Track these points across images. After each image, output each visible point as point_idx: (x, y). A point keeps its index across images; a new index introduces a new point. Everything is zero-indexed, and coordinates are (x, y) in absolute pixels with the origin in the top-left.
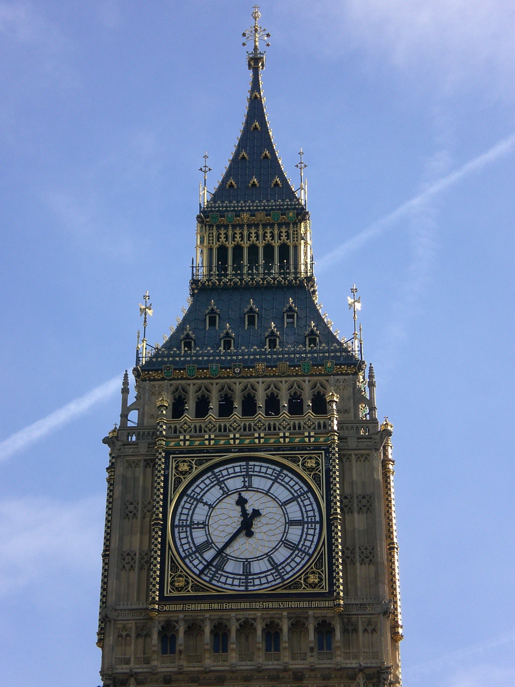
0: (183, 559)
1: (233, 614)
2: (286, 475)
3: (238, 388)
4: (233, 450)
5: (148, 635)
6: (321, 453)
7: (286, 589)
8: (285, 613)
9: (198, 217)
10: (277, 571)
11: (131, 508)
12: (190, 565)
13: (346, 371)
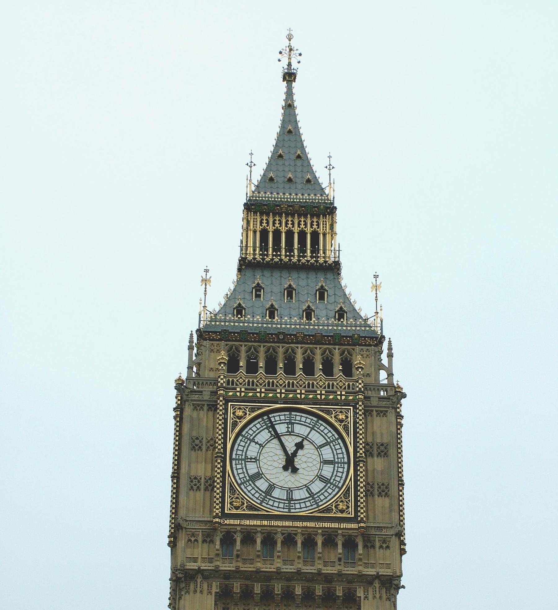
1: (279, 530)
2: (322, 425)
3: (281, 351)
5: (212, 541)
6: (350, 409)
7: (320, 512)
8: (320, 531)
9: (245, 205)
10: (313, 499)
11: (197, 442)
12: (245, 490)
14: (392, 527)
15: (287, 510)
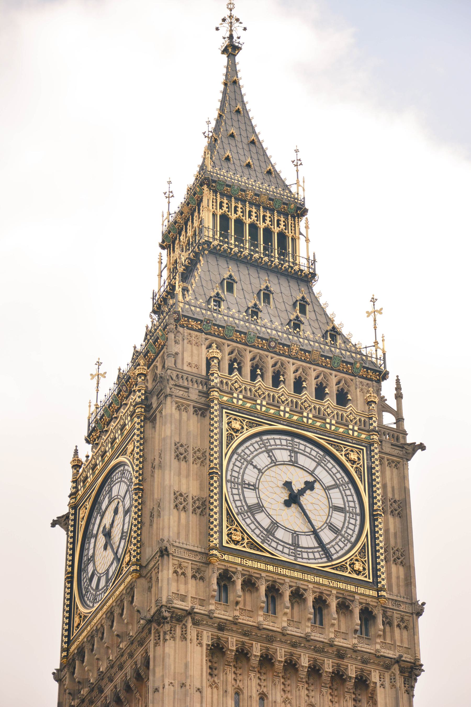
1: (287, 580)
2: (329, 461)
3: (271, 362)
6: (363, 450)
7: (333, 569)
8: (334, 592)
11: (182, 450)
13: (371, 376)
14: (411, 604)
15: (293, 558)
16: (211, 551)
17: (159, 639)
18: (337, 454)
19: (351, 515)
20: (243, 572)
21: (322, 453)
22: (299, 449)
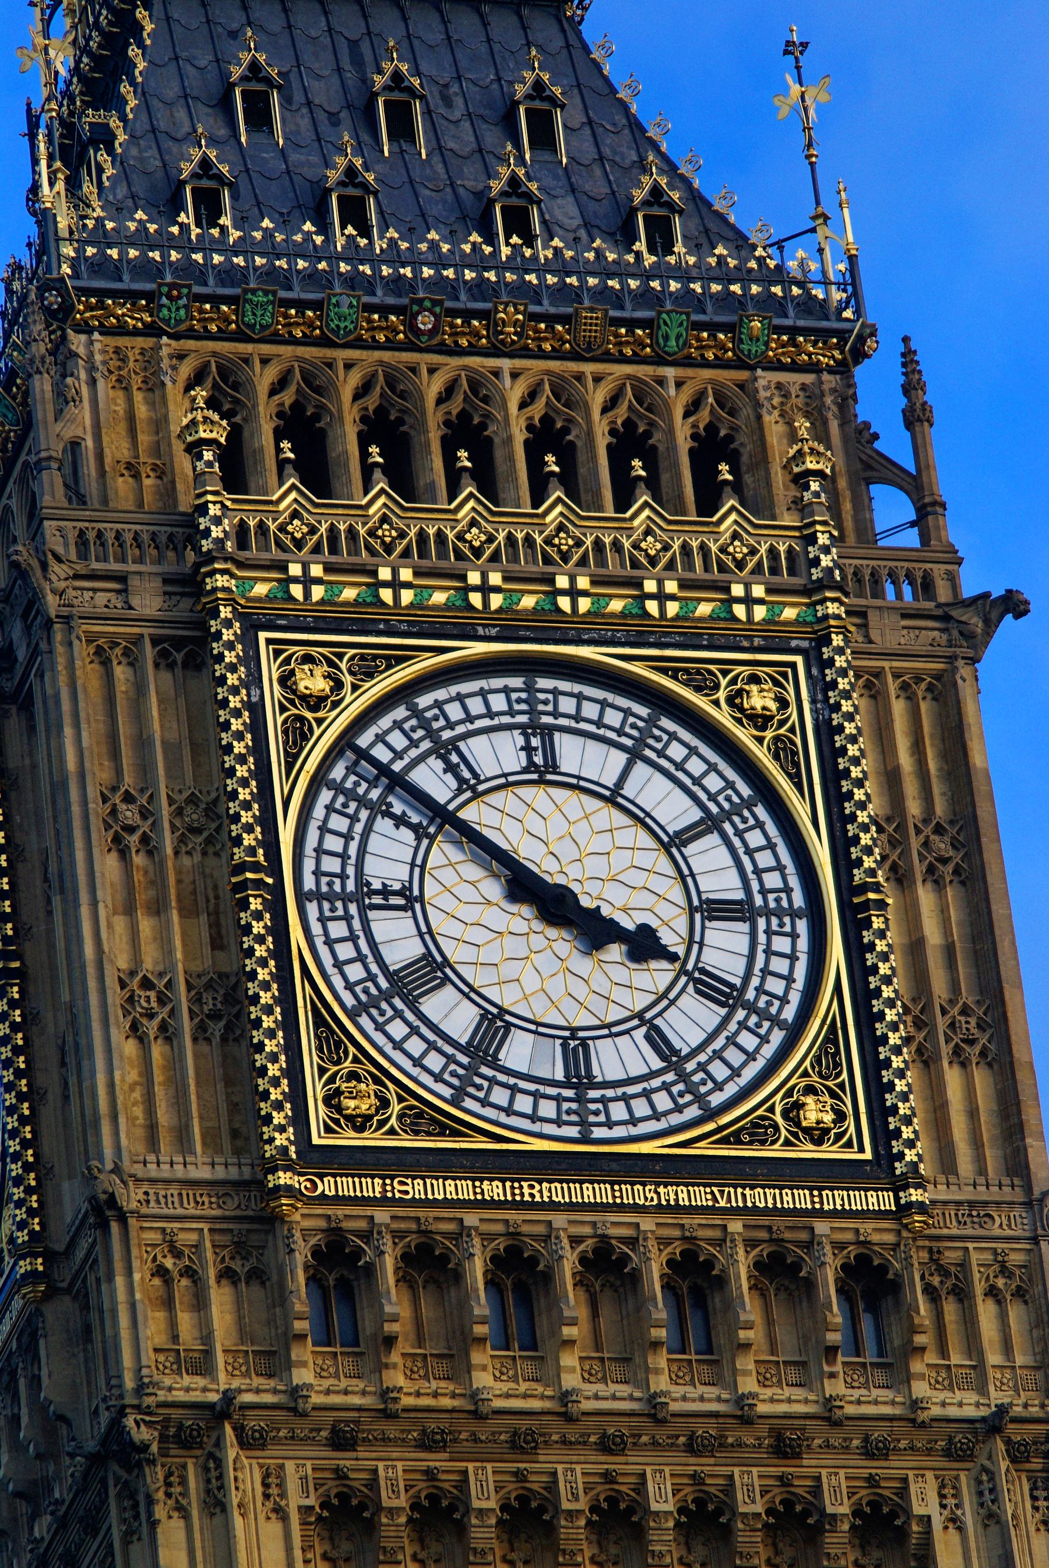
0: (353, 1015)
1: (559, 1220)
2: (673, 736)
4: (481, 631)
10: (683, 1077)
15: (573, 1132)
16: (270, 1177)
17: (137, 1517)
18: (701, 702)
19: (775, 921)
20: (395, 1226)
21: (643, 711)
22: (556, 714)
